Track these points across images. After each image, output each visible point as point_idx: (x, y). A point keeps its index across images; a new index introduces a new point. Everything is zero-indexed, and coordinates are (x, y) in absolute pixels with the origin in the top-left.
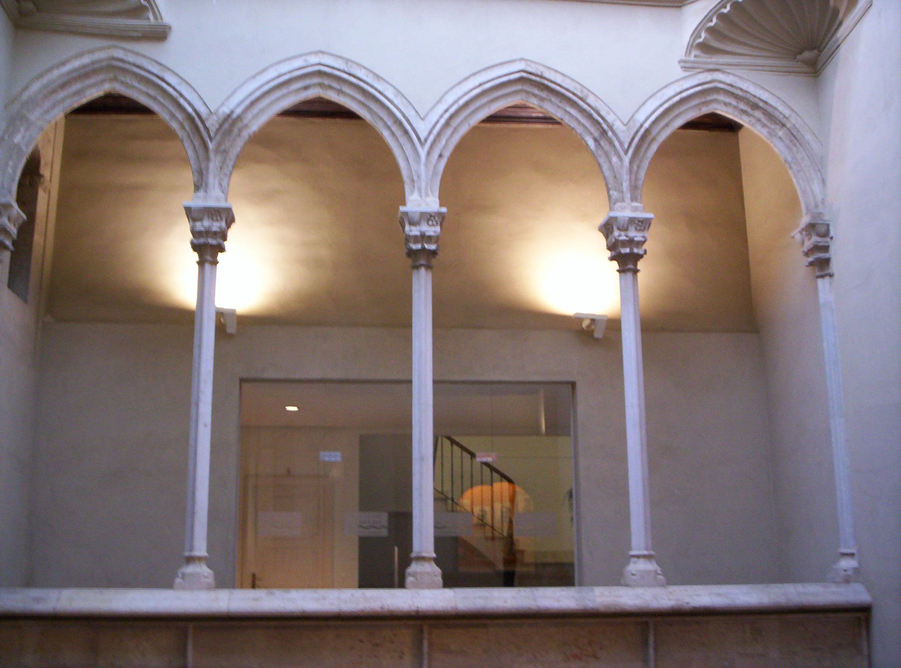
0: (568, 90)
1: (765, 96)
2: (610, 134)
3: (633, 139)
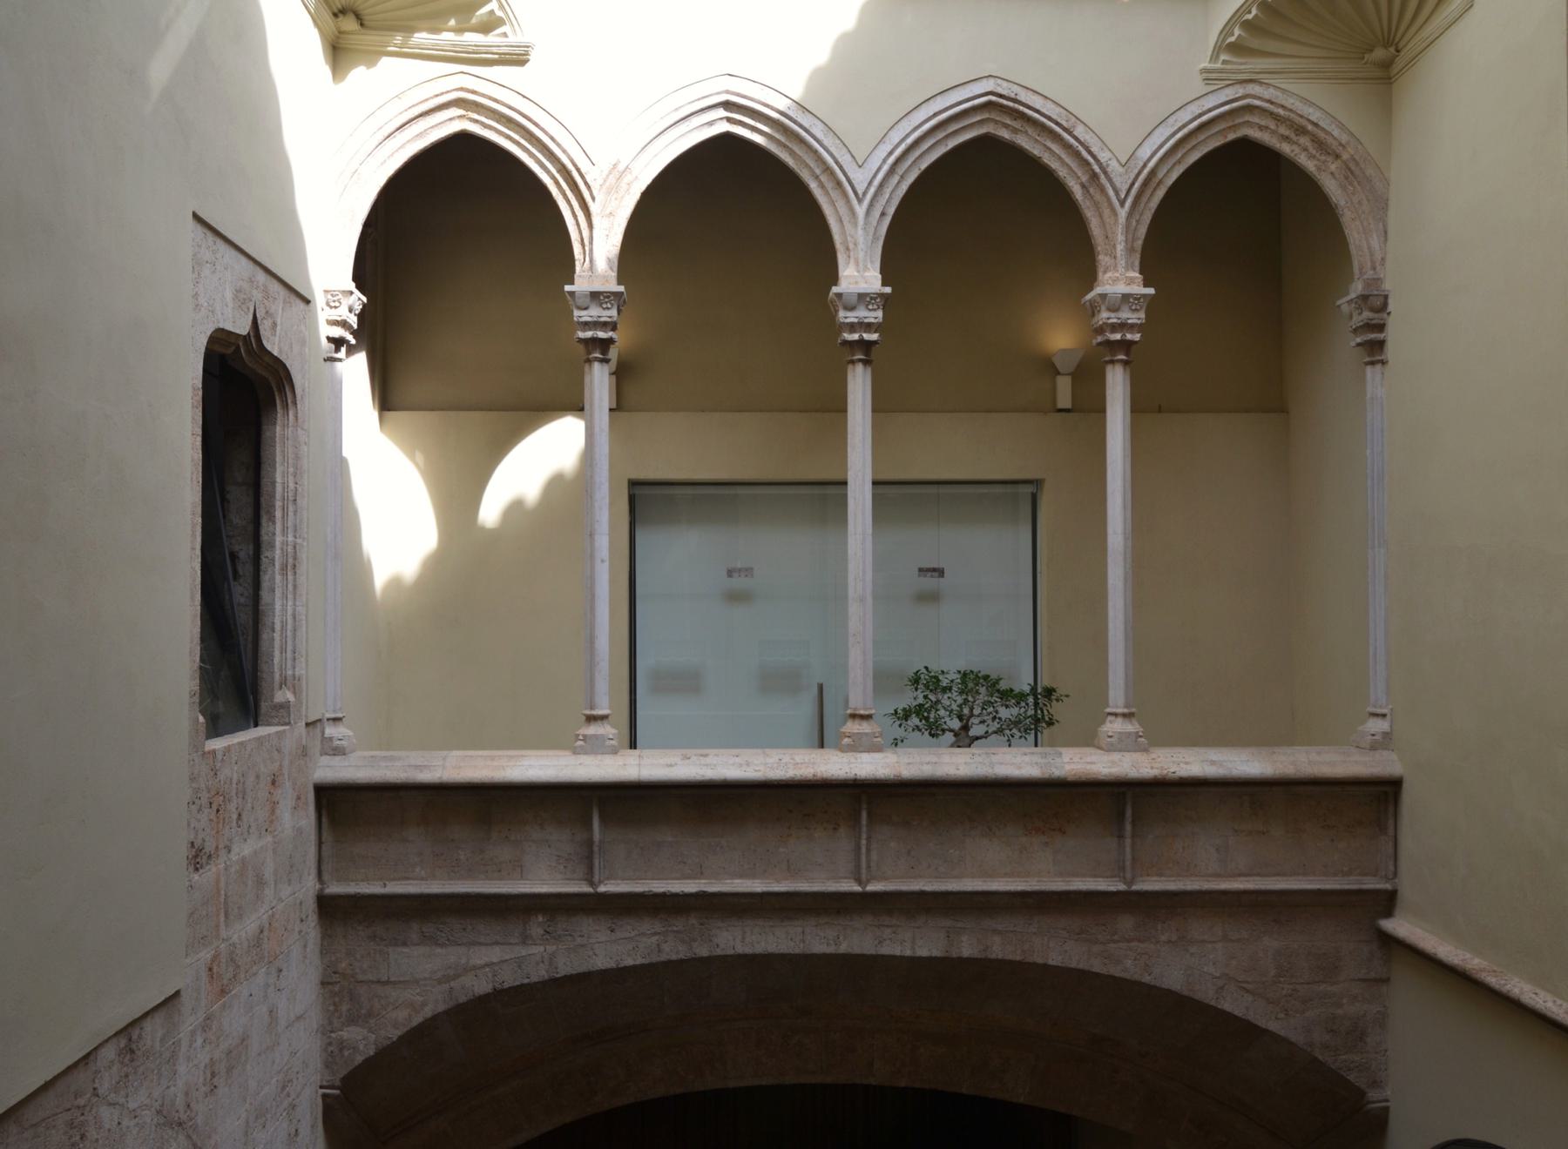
0: (1049, 118)
1: (1315, 115)
3: (1133, 184)
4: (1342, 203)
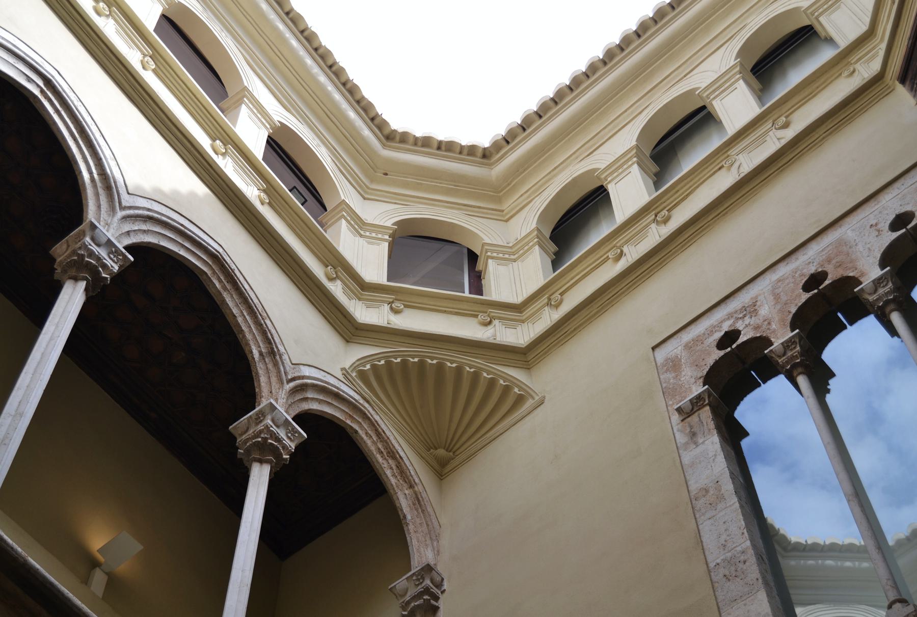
1: (402, 454)
2: (278, 357)
4: (409, 517)
